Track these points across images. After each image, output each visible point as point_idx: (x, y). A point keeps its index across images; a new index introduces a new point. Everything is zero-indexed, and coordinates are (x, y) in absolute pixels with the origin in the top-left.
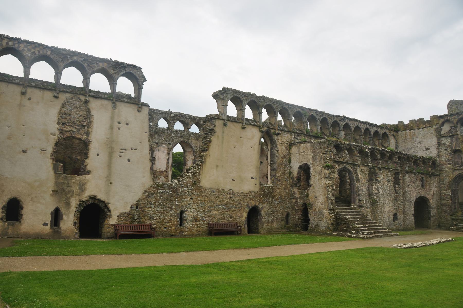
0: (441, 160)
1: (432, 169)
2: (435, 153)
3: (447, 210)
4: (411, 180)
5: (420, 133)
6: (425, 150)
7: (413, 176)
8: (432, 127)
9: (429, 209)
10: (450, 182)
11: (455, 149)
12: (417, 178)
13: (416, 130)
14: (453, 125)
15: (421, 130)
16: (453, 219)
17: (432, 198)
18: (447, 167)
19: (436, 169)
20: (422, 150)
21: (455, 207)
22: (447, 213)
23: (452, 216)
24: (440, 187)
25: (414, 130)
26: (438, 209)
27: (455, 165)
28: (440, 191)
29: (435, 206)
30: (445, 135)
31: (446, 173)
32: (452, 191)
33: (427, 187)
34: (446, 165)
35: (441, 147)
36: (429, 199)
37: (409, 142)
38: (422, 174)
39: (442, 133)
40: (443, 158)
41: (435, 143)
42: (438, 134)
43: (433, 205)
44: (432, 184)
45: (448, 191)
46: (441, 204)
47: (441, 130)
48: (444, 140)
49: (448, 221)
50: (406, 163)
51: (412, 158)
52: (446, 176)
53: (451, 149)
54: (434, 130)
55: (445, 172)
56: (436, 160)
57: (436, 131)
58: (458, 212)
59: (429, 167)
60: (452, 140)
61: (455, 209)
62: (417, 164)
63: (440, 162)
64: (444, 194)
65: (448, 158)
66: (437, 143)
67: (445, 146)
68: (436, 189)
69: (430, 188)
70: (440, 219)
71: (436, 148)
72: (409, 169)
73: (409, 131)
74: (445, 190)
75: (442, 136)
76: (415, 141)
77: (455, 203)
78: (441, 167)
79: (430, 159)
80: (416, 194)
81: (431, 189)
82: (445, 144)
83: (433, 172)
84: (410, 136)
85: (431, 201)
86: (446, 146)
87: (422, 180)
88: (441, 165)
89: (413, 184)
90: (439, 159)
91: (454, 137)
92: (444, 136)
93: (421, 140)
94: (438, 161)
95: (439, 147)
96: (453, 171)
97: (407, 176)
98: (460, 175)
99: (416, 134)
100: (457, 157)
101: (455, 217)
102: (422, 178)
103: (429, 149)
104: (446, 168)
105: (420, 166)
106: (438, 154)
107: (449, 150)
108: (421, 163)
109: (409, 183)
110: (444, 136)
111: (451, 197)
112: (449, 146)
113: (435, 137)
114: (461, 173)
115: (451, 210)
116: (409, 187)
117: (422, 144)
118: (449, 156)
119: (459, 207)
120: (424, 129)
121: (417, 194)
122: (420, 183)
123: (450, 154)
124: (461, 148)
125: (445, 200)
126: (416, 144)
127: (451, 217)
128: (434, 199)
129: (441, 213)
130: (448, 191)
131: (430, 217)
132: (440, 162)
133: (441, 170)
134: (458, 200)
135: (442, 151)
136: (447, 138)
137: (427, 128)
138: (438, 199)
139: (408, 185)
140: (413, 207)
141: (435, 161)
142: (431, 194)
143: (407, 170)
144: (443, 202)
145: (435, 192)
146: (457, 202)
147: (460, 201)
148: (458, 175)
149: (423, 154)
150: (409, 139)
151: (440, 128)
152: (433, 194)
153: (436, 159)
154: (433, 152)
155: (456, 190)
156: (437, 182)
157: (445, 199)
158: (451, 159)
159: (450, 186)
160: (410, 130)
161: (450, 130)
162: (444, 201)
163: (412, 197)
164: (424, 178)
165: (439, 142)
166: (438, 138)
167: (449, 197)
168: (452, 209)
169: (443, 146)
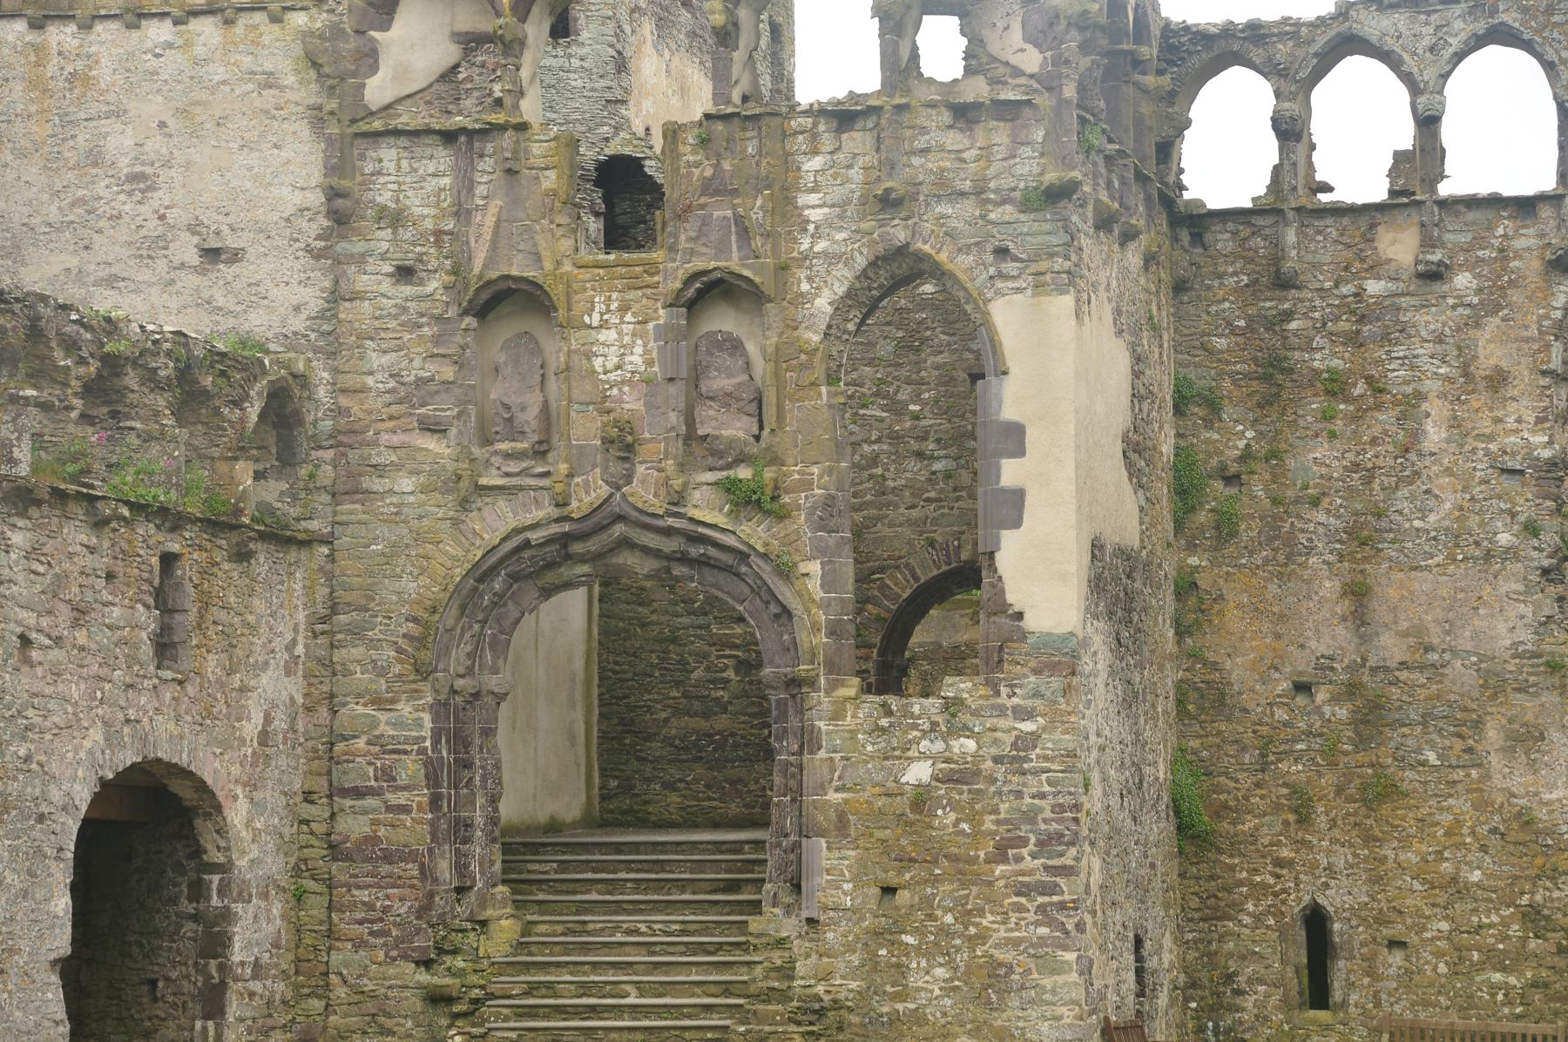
0: (351, 381)
1: (259, 476)
2: (297, 309)
3: (386, 909)
4: (61, 580)
5: (154, 63)
6: (195, 260)
7: (77, 534)
8: (276, 19)
9: (215, 901)
10: (434, 610)
11: (494, 275)
12: (119, 568)
13: (99, 27)
14: (486, 25)
15: (158, 32)
16: (437, 998)
17: (252, 785)
18: (409, 460)
19: (303, 471)
20: (162, 265)
21: (461, 868)
22: (383, 933)
23: (427, 964)
24: (328, 664)
25: (86, 26)
26: (299, 897)
27: (487, 441)
28: (323, 712)
29: (275, 866)
30: (404, 120)
31: (396, 518)
32: (440, 709)
33: (212, 664)
34: (396, 439)
35: (358, 247)
36: (220, 795)
37: (21, 154)
38: (170, 519)
39: (378, 89)
40: (377, 360)
41: (298, 198)
42: (333, 105)
43: (255, 852)
44: (253, 629)
45: (405, 709)
46: (335, 850)
47: (369, 59)
48: (390, 166)
49: (389, 1023)
50: (14, 399)
51: (71, 346)
52: (394, 550)
53: (455, 272)
54: (298, 50)
55: (386, 507)
56: (302, 379)
57: (315, 65)
58: (484, 923)
59: (239, 451)
60: (466, 184)
61: (461, 890)
62: (114, 415)
63: (344, 401)
64: (361, 743)
65: (418, 368)
66: (316, 199)
67: (395, 240)
68: (293, 688)
69: (236, 681)
70: (317, 1005)
71: (308, 249)
72: (36, 468)
73: (20, 26)
74: (378, 702)
75: (377, 125)
76: (95, 158)
77: (461, 830)
78: (353, 456)
79: (253, 369)
80: (97, 735)
81: (243, 689)
82: (395, 218)
83: (265, 509)
84: (38, 85)
85: (237, 814)
86: (407, 234)
87: (164, 599)
88: (347, 436)
89: (76, 624)
90: (336, 371)
91: (489, 148)
92: (397, 133)
93: (156, 145)
94: (322, 393)
95: (342, 247)
96: (464, 504)
97: (17, 538)
98: (527, 544)
99: (105, 73)
100: (502, 358)
101: (461, 973)
102: (168, 560)
103: (236, 256)
104: (397, 467)
105: (148, 438)
106: (321, 316)
107: (433, 285)
108: (161, 401)
109: (30, 618)
110: (393, 123)
111: (433, 779)
112: (438, 243)
113: (304, 130)
114: (535, 526)
115: (423, 911)
116: (35, 655)
117: (159, 198)
118: (437, 340)
119: (498, 867)
120: (196, 25)
121: (112, 739)
122: (148, 619)
123: (438, 319)
124: (548, 265)
125: (370, 802)
126: (100, 188)
127: (423, 977)
128: (270, 795)
129: (330, 934)
130: (405, 709)
131: (223, 985)
132: (344, 401)
133: (348, 490)
134: (494, 800)
135: (364, 282)
136: (418, 150)
137: (229, 22)
138: (308, 797)
139: (25, 641)
140: (61, 875)
141: (297, 391)
142: (242, 741)
143: (23, 470)
144: (354, 826)
145: (280, 723)
146: (479, 820)
147: (509, 810)
148: (504, 540)
149: (174, 303)
150: (19, 128)
151: (352, 43)
152: (264, 737)
153: (301, 366)
154: (274, 293)
155: (477, 695)
156: (301, 616)
157: (371, 792)
158: (448, 372)
159: (425, 655)
160: (37, 25)
161: (455, 68)
162: (365, 812)
163: (54, 767)
164: (186, 570)
165: (346, 184)
166: (330, 141)
167: (410, 769)
168: (431, 895)
169: (383, 239)
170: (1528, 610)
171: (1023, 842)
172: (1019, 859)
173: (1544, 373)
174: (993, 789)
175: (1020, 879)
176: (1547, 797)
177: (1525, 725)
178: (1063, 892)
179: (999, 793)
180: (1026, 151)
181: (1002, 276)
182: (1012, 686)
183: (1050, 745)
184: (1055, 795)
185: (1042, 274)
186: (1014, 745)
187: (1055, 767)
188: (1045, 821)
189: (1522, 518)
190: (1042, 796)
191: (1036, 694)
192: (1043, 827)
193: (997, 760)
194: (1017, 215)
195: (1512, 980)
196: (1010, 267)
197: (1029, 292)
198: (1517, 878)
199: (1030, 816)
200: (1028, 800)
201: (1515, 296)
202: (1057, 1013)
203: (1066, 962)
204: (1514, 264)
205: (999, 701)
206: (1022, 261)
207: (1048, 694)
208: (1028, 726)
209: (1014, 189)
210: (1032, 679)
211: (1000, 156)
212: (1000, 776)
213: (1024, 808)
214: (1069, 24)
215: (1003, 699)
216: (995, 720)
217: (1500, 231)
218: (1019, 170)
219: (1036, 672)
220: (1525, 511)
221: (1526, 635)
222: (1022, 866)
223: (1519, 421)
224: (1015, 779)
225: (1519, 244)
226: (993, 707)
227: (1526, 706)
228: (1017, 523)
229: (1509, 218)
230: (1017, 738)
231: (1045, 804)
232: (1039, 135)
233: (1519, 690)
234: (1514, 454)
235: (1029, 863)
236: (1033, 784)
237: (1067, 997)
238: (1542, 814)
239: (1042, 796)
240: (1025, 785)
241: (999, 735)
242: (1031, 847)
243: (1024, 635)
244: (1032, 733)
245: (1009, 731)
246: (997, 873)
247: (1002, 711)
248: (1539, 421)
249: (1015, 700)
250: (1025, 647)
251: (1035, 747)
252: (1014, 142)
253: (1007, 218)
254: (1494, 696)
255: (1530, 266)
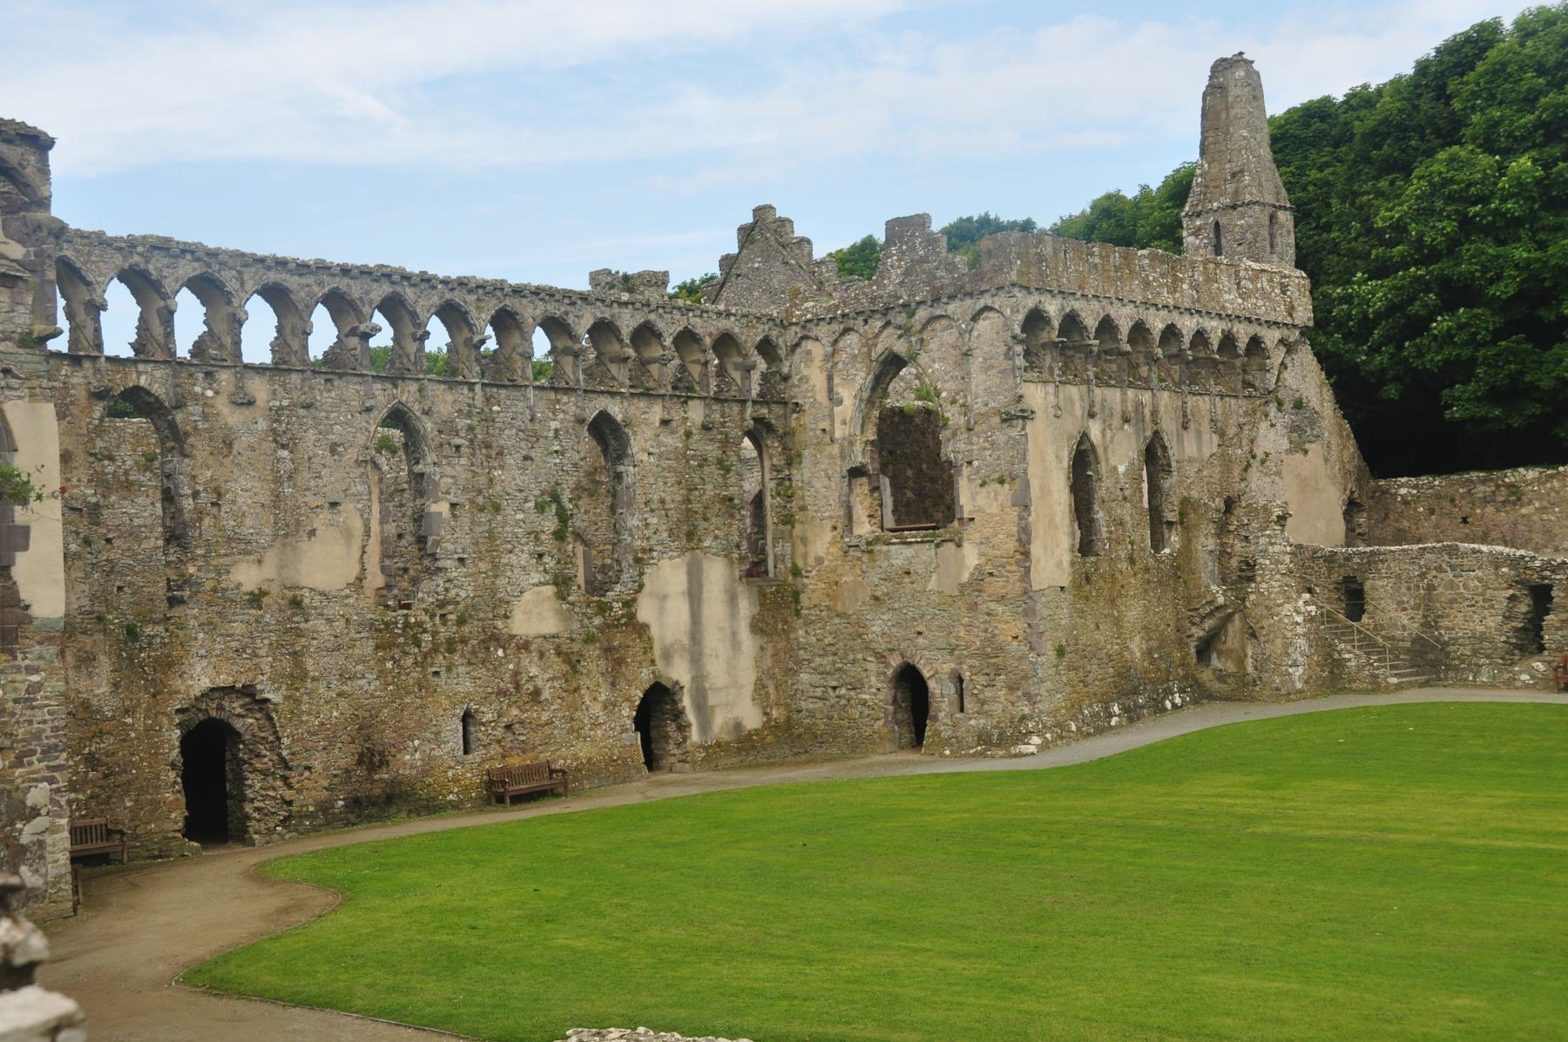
170: (86, 588)
171: (33, 752)
172: (30, 764)
173: (91, 455)
174: (14, 720)
175: (31, 776)
176: (97, 692)
177: (86, 652)
178: (58, 782)
179: (18, 722)
180: (21, 309)
181: (9, 387)
182: (25, 653)
183: (49, 689)
184: (53, 721)
185: (34, 388)
186: (27, 691)
187: (53, 703)
188: (47, 738)
189: (82, 536)
190: (45, 722)
191: (41, 657)
192: (46, 741)
193: (16, 701)
194: (16, 350)
195: (81, 796)
196: (14, 382)
197: (27, 399)
198: (81, 738)
199: (37, 736)
200: (36, 726)
201: (74, 410)
202: (55, 859)
203: (62, 825)
204: (72, 392)
205: (17, 663)
206: (21, 379)
207: (48, 656)
208: (35, 678)
209: (13, 332)
210: (37, 647)
211: (5, 310)
212: (18, 711)
213: (34, 731)
214: (49, 233)
215: (19, 662)
216: (13, 675)
217: (63, 372)
218: (17, 321)
219: (40, 643)
220: (84, 531)
221: (85, 602)
222: (32, 768)
223: (79, 481)
224: (28, 712)
225: (74, 380)
226: (13, 667)
227: (86, 642)
228: (25, 548)
229: (68, 365)
230: (29, 686)
231: (47, 727)
232: (29, 300)
233: (82, 633)
234: (77, 499)
235: (37, 765)
236: (39, 715)
237: (62, 847)
238: (95, 702)
239: (45, 722)
240: (34, 716)
241: (17, 685)
242: (38, 755)
243: (31, 620)
244: (38, 682)
245: (23, 682)
246: (17, 774)
247: (18, 669)
248: (89, 481)
249: (27, 662)
250: (32, 628)
251: (40, 691)
252: (13, 302)
253: (11, 350)
254: (70, 637)
255: (80, 394)
